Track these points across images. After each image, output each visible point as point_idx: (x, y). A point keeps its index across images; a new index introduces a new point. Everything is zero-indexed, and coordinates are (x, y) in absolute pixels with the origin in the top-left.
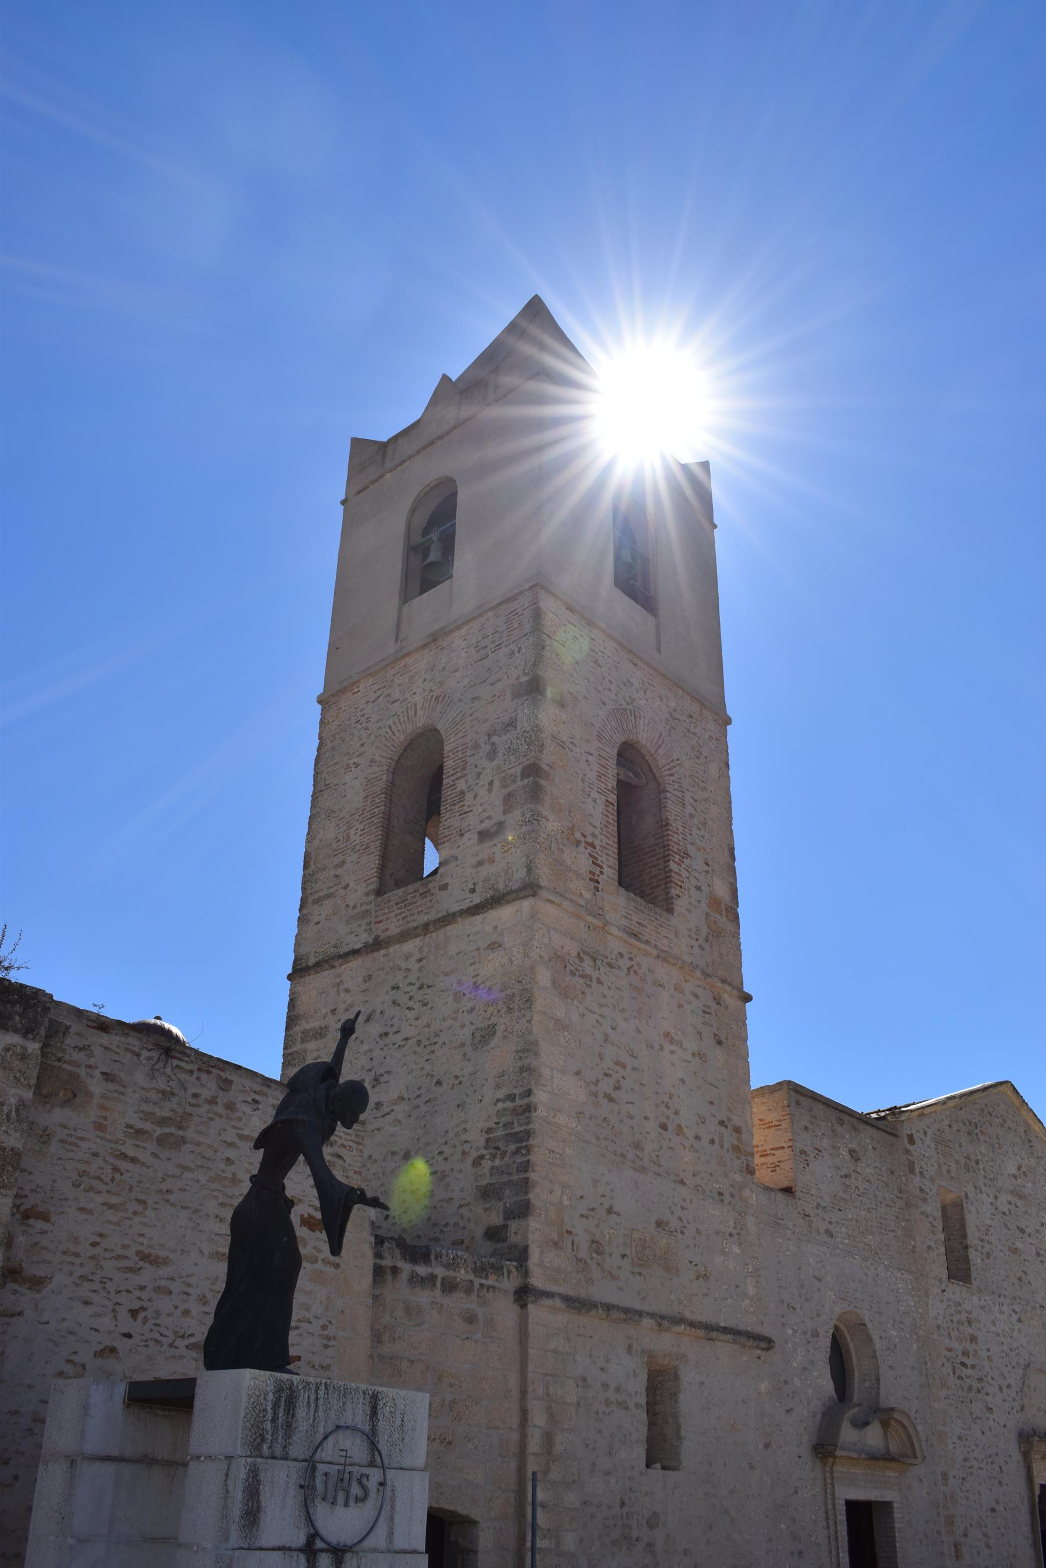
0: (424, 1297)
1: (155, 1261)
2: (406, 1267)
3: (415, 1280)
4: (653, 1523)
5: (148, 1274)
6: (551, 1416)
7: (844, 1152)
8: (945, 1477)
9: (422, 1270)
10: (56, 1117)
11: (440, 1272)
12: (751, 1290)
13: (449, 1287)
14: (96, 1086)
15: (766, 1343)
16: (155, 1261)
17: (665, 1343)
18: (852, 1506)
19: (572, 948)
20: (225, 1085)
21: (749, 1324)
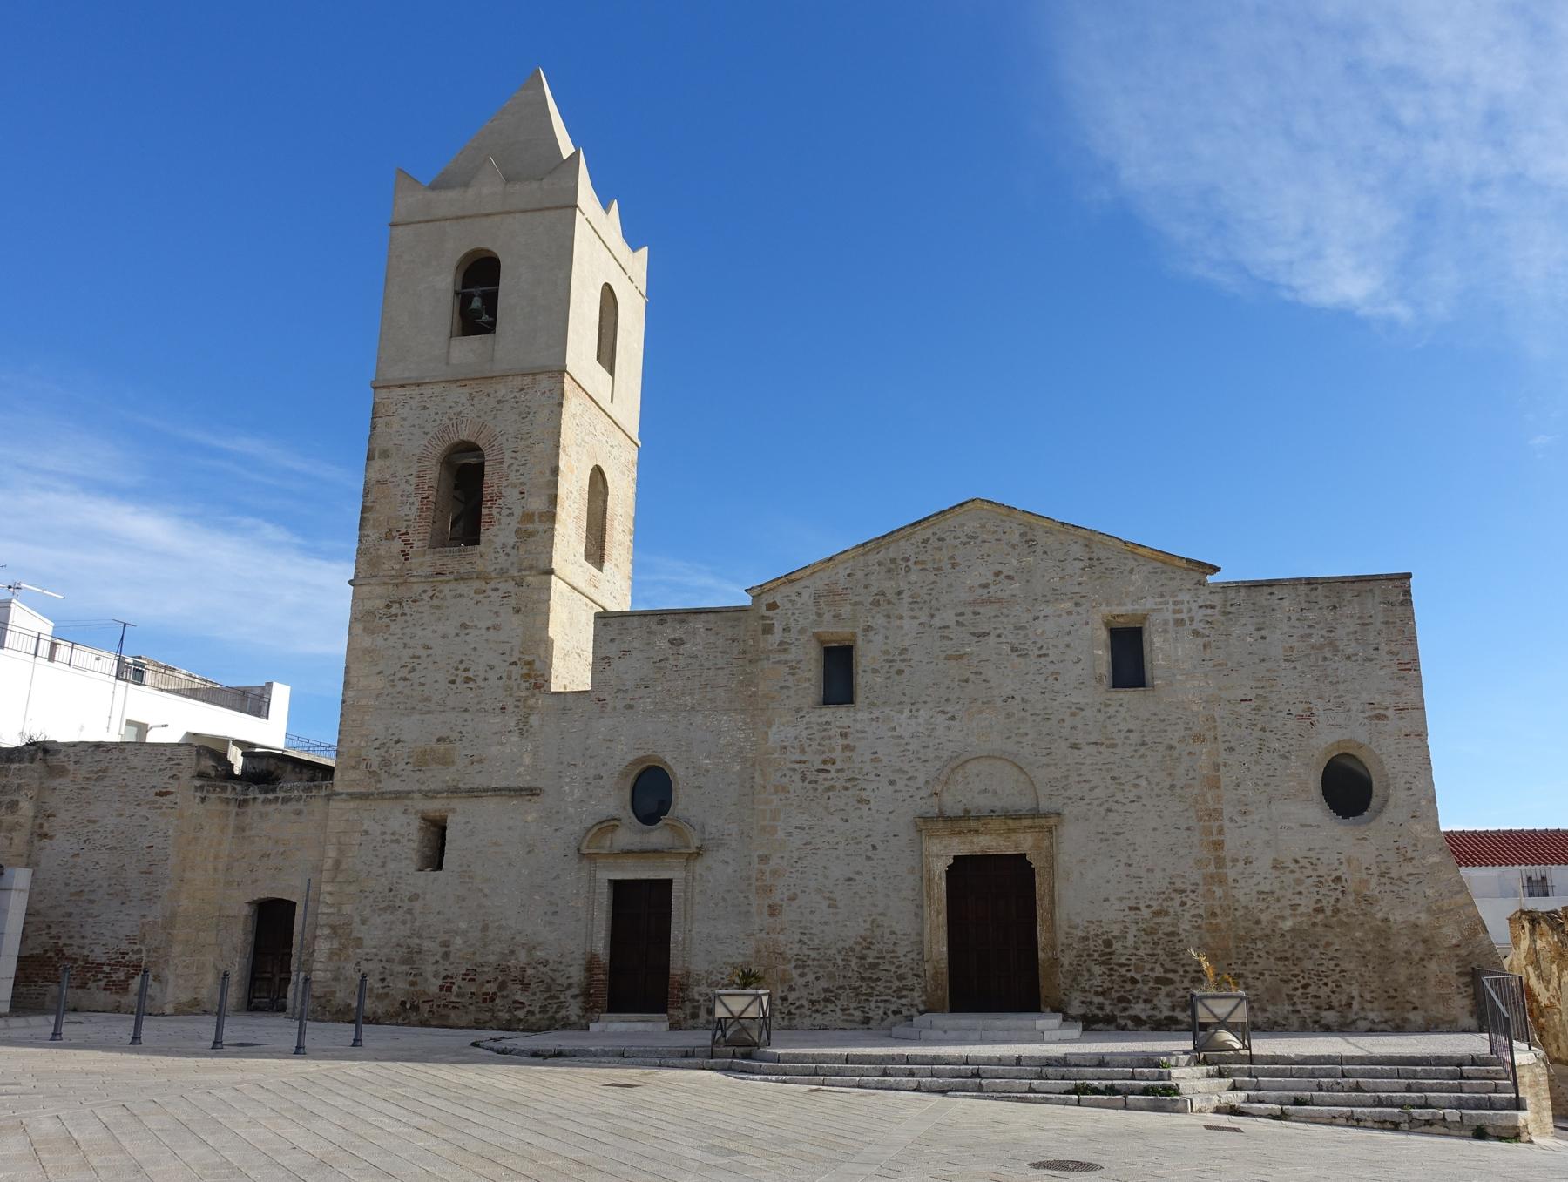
0: (271, 808)
1: (94, 822)
2: (261, 797)
3: (265, 801)
4: (414, 898)
5: (91, 827)
6: (340, 851)
7: (664, 644)
8: (764, 859)
9: (271, 796)
10: (57, 782)
11: (281, 795)
12: (527, 760)
13: (286, 800)
14: (71, 767)
15: (533, 792)
16: (94, 822)
17: (434, 807)
18: (618, 886)
19: (380, 604)
20: (123, 751)
21: (525, 780)
